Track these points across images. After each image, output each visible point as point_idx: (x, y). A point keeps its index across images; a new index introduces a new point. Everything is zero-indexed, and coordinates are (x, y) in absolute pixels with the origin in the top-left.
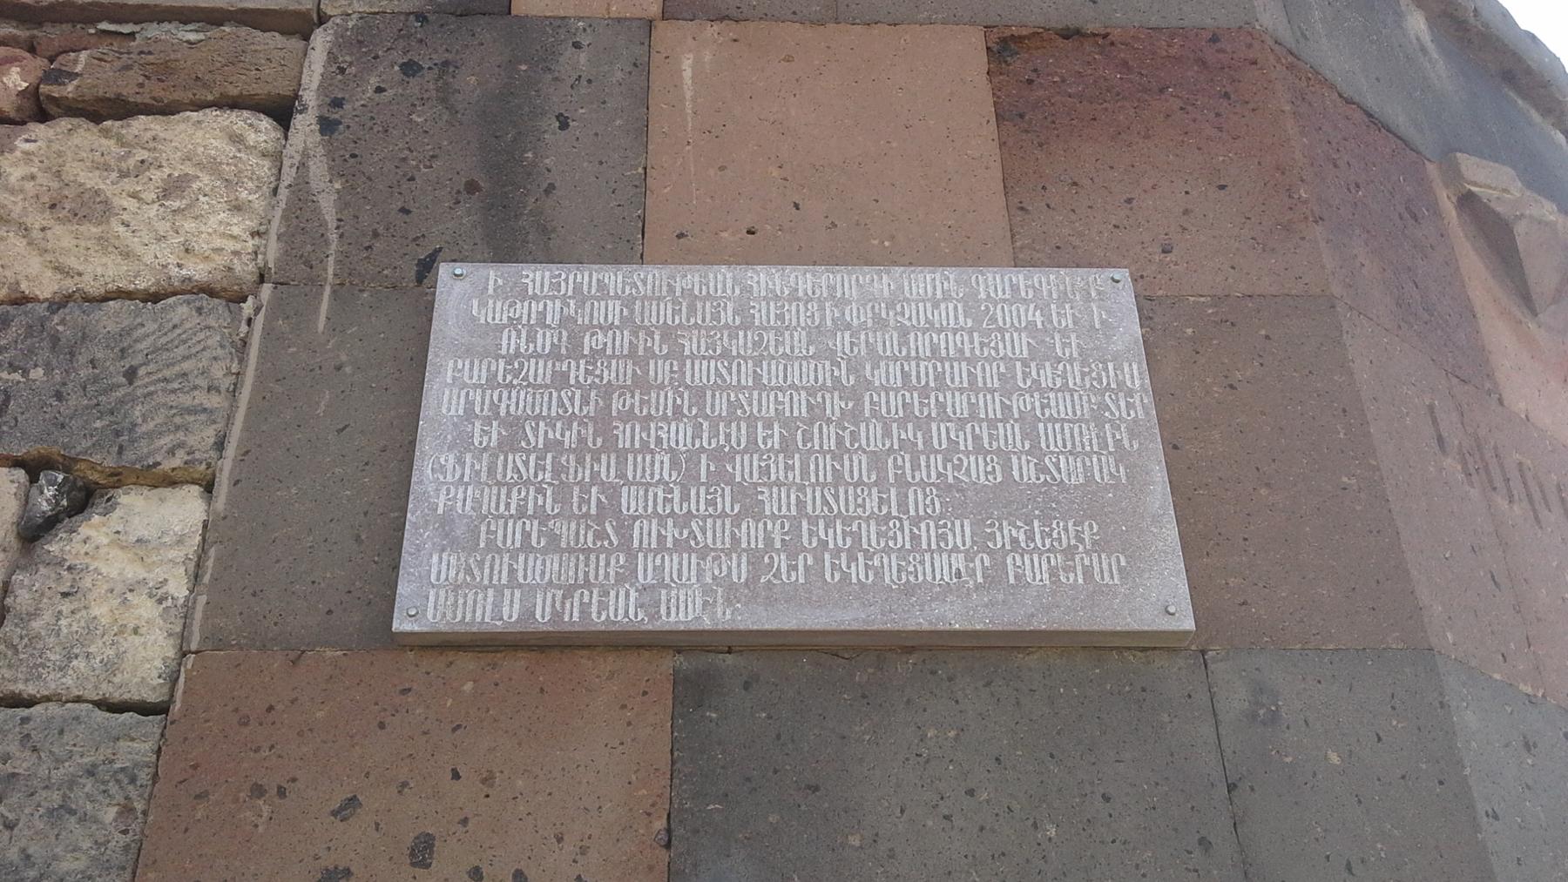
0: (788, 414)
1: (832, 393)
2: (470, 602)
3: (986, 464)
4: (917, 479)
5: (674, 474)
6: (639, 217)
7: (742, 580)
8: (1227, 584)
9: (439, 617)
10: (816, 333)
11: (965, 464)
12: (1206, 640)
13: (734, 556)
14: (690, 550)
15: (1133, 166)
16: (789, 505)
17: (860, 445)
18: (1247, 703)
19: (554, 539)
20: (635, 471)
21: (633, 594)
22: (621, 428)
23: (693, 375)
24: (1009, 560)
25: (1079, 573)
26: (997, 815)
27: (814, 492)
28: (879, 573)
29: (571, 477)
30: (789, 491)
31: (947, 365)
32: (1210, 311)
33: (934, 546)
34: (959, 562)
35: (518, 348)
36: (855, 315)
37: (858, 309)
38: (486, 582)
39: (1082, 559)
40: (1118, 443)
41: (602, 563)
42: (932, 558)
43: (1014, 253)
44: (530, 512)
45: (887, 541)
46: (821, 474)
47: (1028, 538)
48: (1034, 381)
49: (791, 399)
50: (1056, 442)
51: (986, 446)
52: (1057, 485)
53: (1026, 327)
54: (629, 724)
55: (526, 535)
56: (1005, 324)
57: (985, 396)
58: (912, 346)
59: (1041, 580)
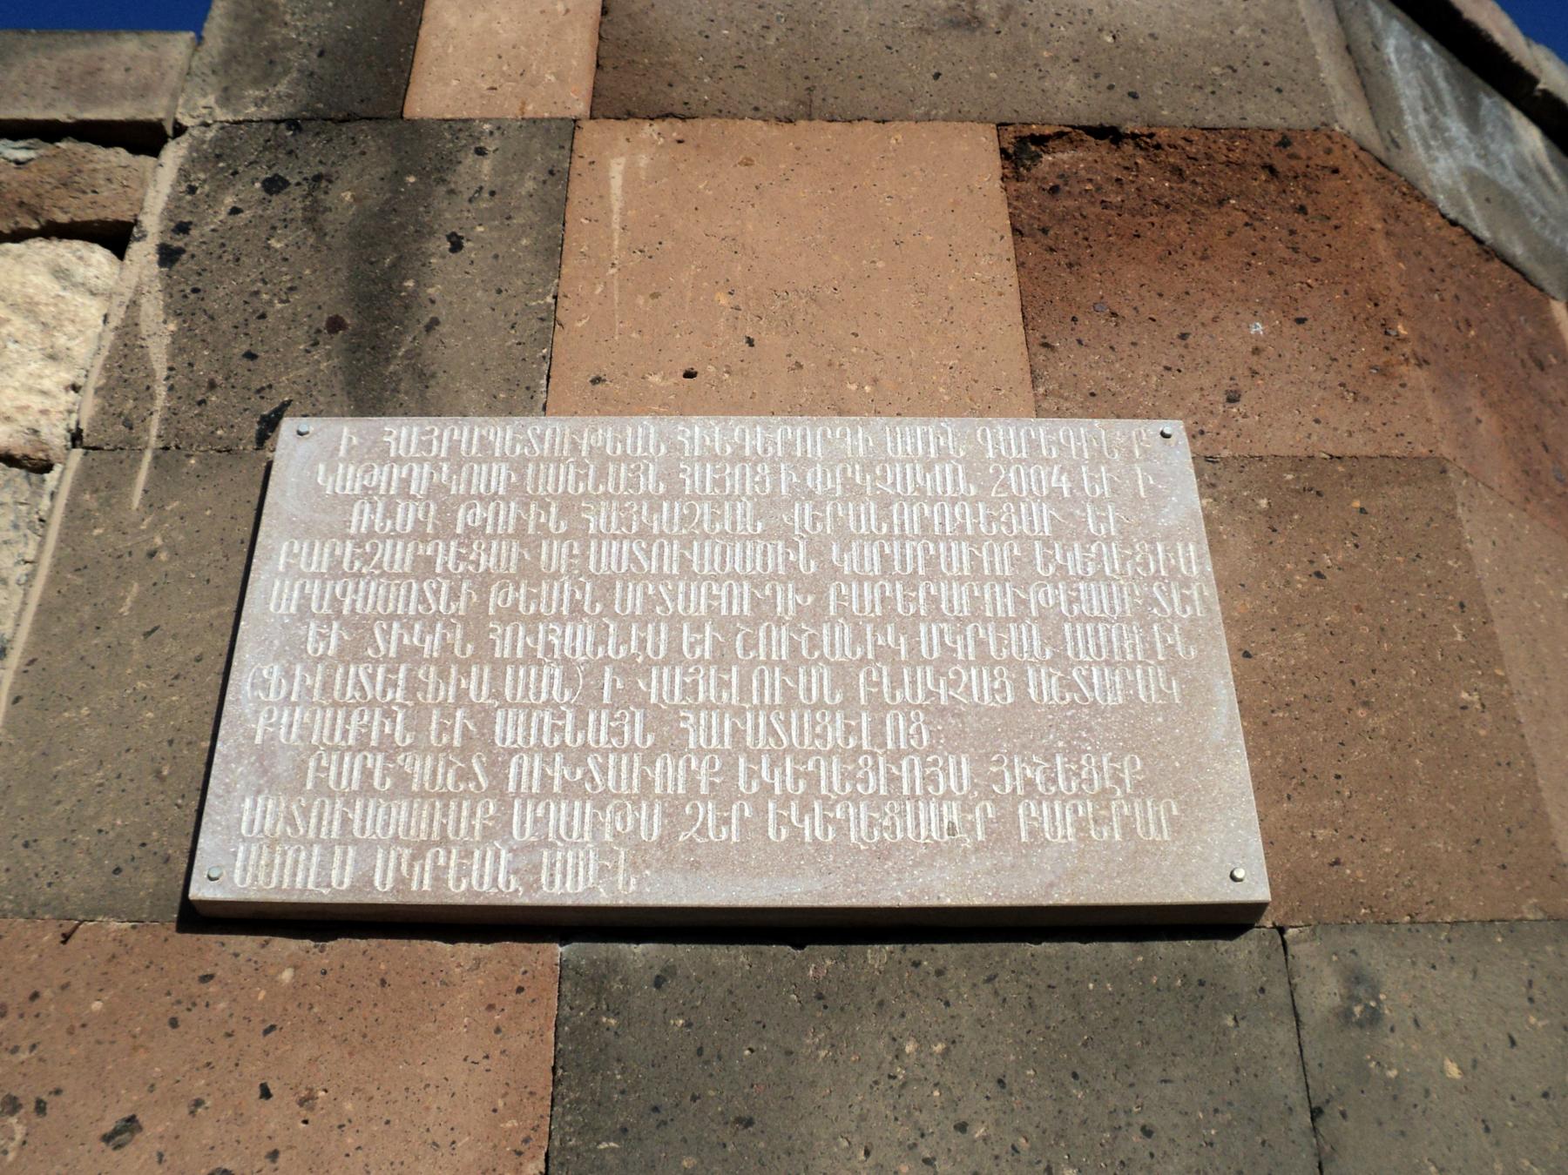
0: (724, 612)
1: (785, 584)
2: (289, 862)
3: (993, 679)
5: (567, 694)
6: (544, 357)
7: (654, 838)
8: (1313, 837)
9: (249, 881)
10: (768, 505)
11: (965, 678)
12: (1286, 914)
13: (644, 805)
14: (585, 797)
15: (1187, 293)
17: (822, 656)
18: (1338, 999)
19: (403, 779)
20: (515, 688)
22: (499, 631)
23: (599, 561)
26: (997, 1157)
27: (757, 717)
28: (842, 829)
29: (429, 696)
31: (942, 546)
34: (952, 813)
35: (372, 524)
36: (819, 479)
37: (824, 472)
38: (311, 835)
39: (1121, 807)
40: (1170, 649)
41: (465, 813)
43: (1036, 401)
44: (373, 743)
45: (855, 785)
46: (767, 693)
47: (1048, 779)
48: (1059, 568)
50: (1088, 649)
52: (1089, 707)
53: (1048, 497)
54: (498, 1030)
55: (367, 774)
56: (1020, 491)
57: (993, 587)
59: (1065, 837)
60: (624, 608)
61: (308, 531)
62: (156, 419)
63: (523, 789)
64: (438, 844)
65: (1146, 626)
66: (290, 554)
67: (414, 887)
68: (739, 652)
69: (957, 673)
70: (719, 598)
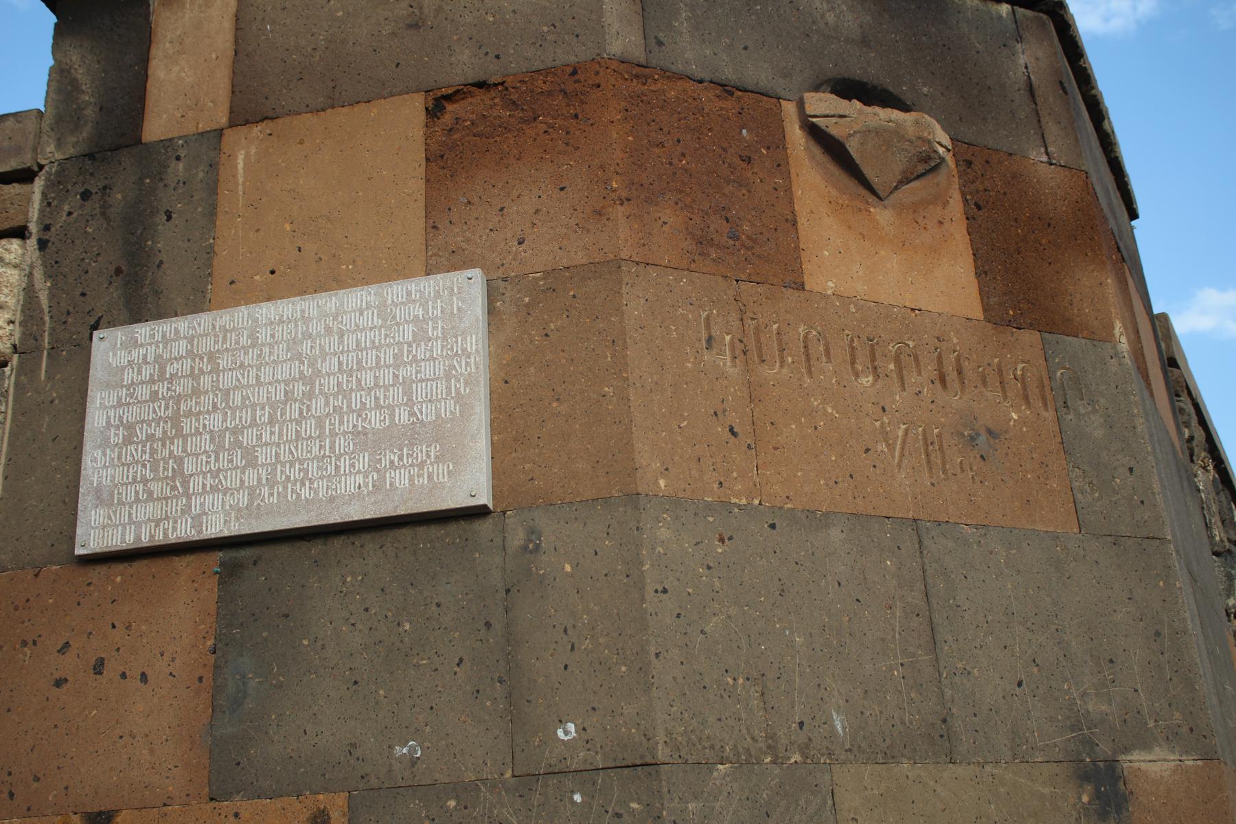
0: (273, 399)
2: (110, 535)
3: (381, 415)
4: (342, 430)
9: (96, 544)
11: (369, 417)
13: (241, 492)
16: (271, 457)
17: (312, 414)
19: (150, 493)
21: (189, 520)
23: (223, 382)
24: (388, 475)
25: (426, 476)
29: (159, 455)
30: (271, 447)
32: (541, 283)
33: (347, 472)
34: (360, 479)
38: (118, 522)
40: (457, 390)
41: (174, 505)
42: (346, 479)
44: (139, 480)
47: (399, 459)
49: (276, 389)
51: (382, 403)
53: (413, 320)
54: (196, 590)
56: (400, 319)
58: (346, 343)
60: (233, 404)
61: (108, 386)
62: (46, 333)
63: (196, 491)
64: (165, 519)
65: (448, 381)
66: (102, 398)
67: (157, 538)
68: (279, 417)
69: (366, 414)
70: (271, 392)
